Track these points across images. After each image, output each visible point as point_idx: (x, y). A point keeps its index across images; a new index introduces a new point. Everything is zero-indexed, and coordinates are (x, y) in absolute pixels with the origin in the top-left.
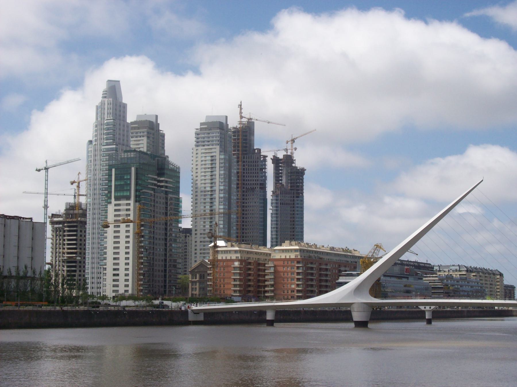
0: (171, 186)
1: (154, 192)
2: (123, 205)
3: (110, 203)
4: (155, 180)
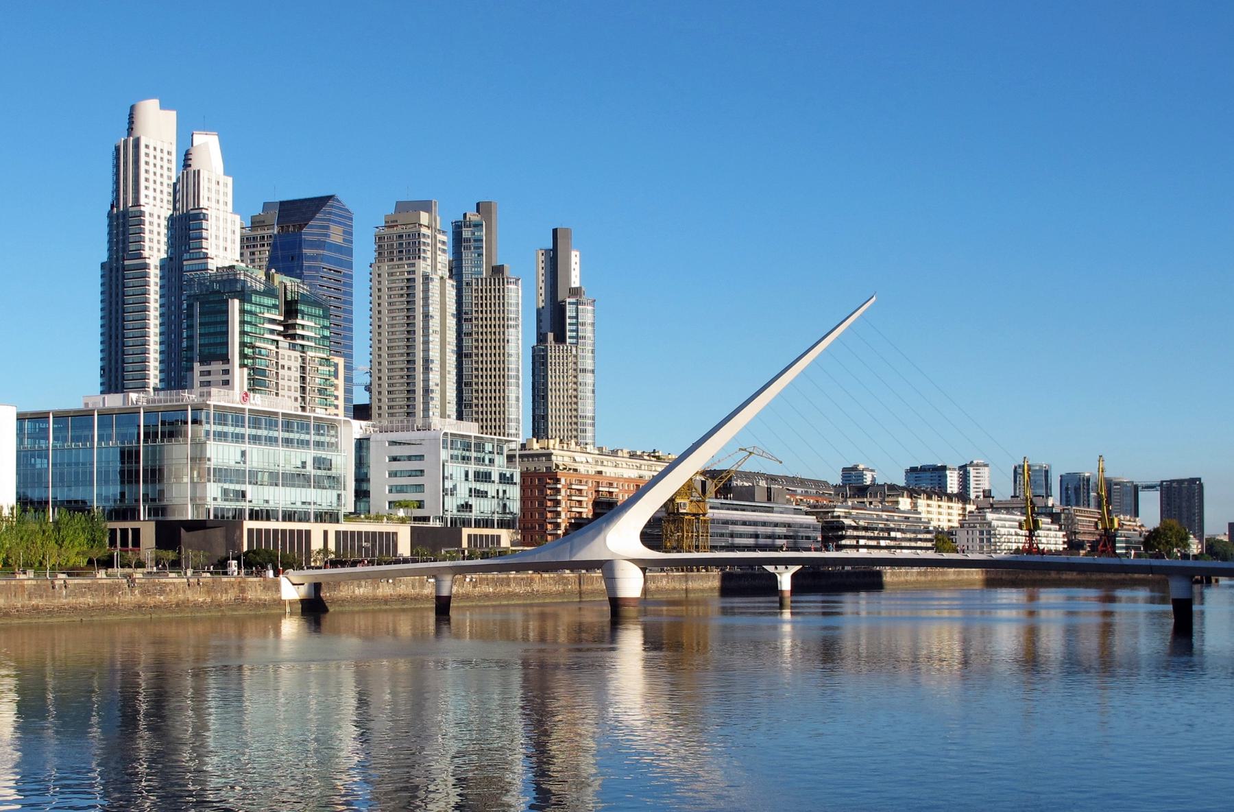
0: (312, 334)
1: (277, 348)
2: (217, 373)
3: (192, 369)
4: (279, 323)
